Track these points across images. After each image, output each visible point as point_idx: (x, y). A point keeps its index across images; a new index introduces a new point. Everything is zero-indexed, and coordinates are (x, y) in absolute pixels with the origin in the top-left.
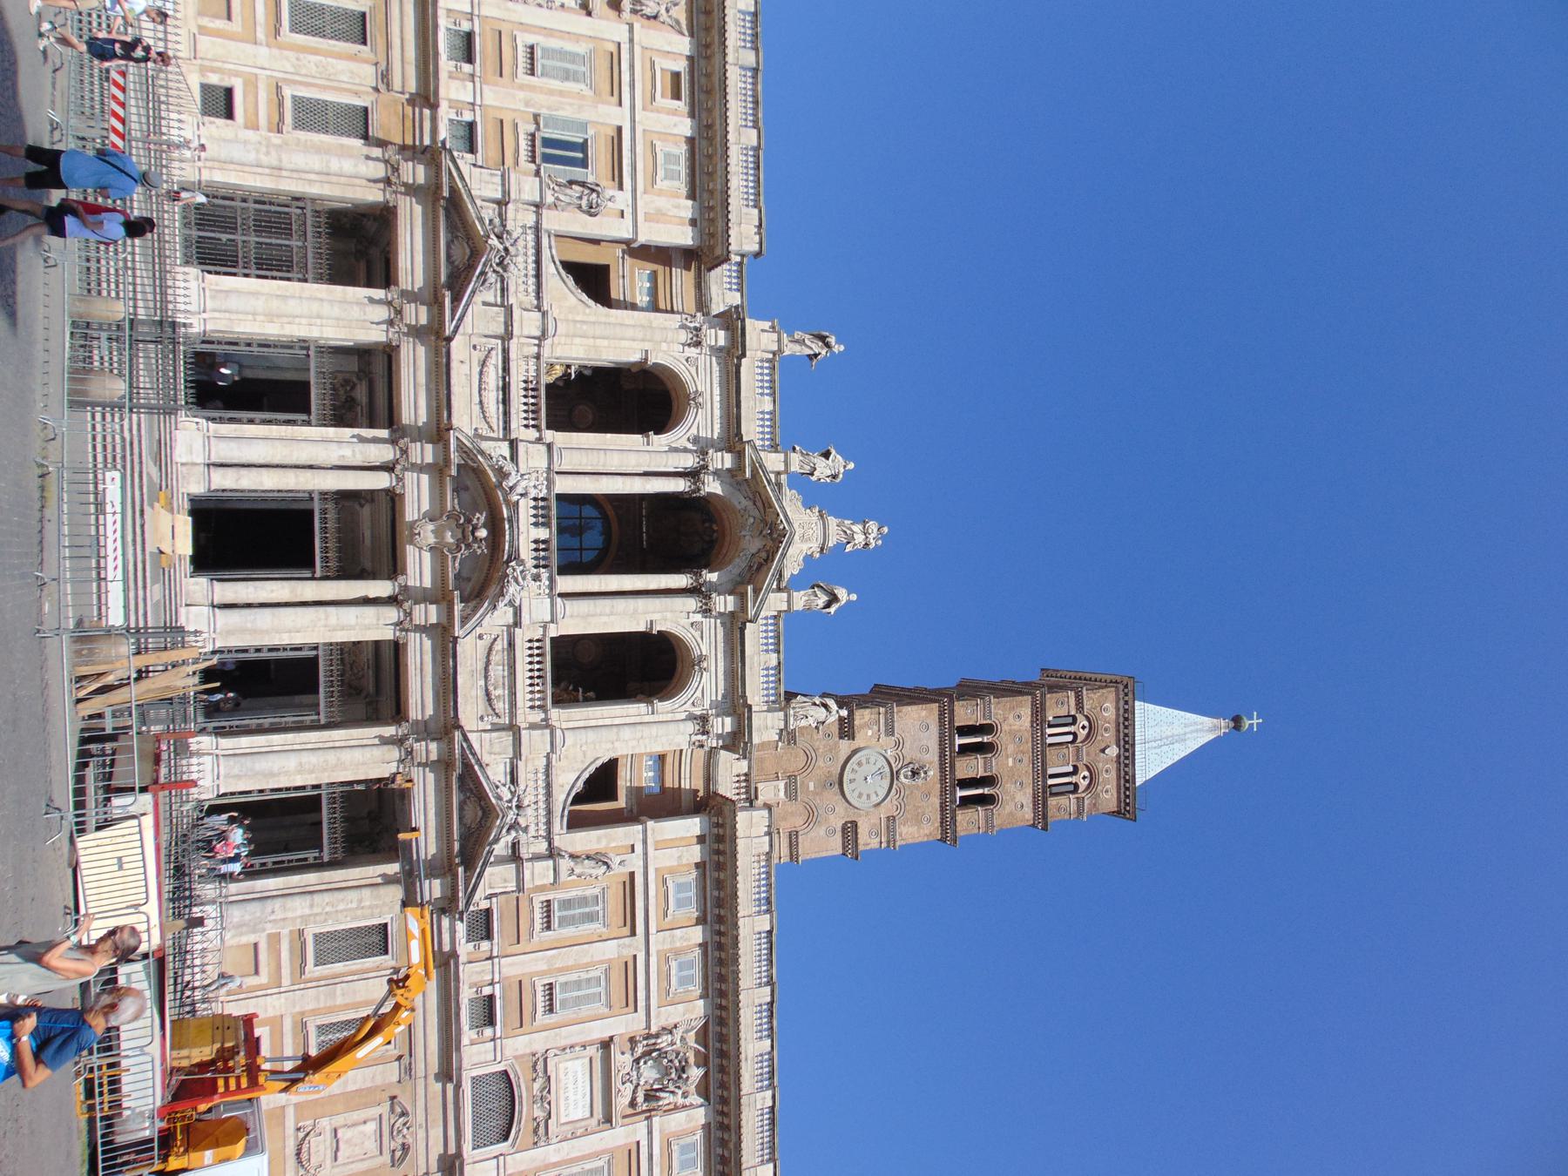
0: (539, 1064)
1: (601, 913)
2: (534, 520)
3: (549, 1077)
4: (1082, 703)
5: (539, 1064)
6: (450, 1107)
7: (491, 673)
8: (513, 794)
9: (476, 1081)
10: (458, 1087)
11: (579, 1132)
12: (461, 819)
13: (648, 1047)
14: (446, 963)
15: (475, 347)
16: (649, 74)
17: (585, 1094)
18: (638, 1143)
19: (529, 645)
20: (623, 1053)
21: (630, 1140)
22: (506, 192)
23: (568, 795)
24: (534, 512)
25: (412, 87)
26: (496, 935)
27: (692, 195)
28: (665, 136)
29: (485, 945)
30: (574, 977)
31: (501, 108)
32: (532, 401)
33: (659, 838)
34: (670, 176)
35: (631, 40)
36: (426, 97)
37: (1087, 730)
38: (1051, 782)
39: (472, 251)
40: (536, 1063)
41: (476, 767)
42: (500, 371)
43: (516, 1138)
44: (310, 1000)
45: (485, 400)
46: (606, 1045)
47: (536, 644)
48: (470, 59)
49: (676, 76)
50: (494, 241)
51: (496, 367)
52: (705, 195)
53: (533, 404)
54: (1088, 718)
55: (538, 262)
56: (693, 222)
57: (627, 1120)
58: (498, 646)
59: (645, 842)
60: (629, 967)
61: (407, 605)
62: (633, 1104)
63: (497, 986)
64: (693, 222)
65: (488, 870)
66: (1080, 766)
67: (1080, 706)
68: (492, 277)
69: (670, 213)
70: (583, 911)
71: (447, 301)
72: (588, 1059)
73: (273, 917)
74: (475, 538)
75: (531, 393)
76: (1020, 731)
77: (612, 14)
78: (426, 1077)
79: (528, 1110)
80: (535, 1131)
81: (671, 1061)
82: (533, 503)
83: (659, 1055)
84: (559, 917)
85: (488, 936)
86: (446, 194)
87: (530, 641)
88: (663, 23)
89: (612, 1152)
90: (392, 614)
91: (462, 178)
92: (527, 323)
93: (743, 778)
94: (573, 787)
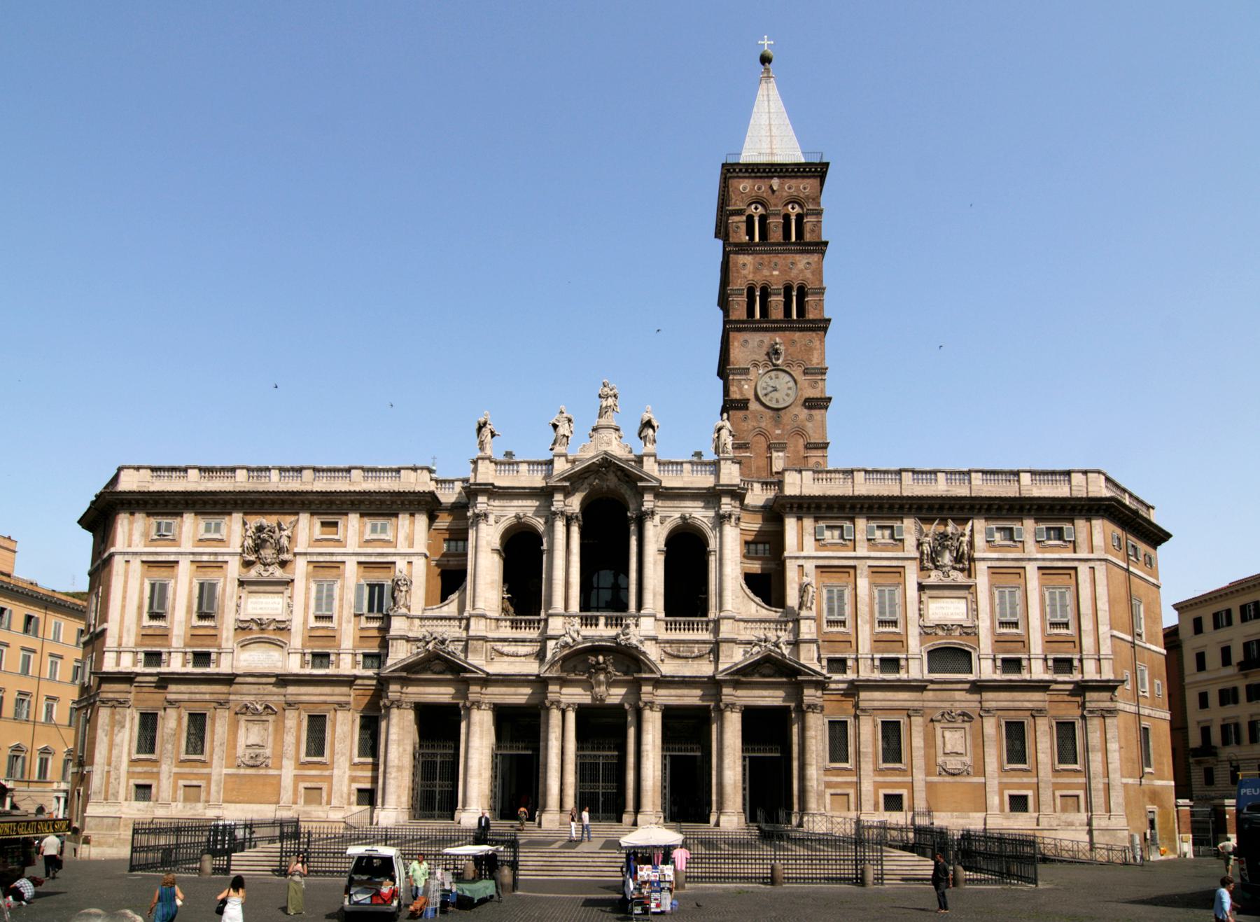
0: (926, 632)
1: (839, 588)
2: (594, 627)
3: (937, 625)
4: (738, 210)
5: (926, 632)
6: (944, 686)
7: (684, 654)
8: (756, 645)
9: (930, 671)
10: (932, 682)
11: (975, 607)
12: (769, 676)
13: (929, 560)
14: (854, 689)
15: (492, 659)
16: (324, 543)
17: (952, 603)
18: (988, 567)
19: (669, 631)
20: (930, 576)
21: (986, 573)
22: (402, 638)
23: (763, 607)
24: (589, 627)
25: (345, 690)
26: (844, 656)
27: (396, 515)
28: (362, 533)
29: (850, 663)
30: (876, 608)
31: (354, 638)
32: (523, 624)
33: (796, 548)
34: (384, 530)
35: (305, 554)
36: (349, 681)
37: (760, 207)
38: (793, 239)
39: (437, 659)
40: (927, 634)
41: (739, 666)
42: (506, 644)
43: (971, 647)
44: (867, 766)
45: (523, 653)
46: (921, 587)
47: (669, 626)
48: (328, 655)
49: (324, 524)
50: (430, 646)
51: (503, 646)
52: (395, 507)
53: (526, 624)
54: (750, 205)
55: (442, 618)
56: (412, 515)
57: (973, 575)
58: (669, 650)
59: (797, 558)
60: (875, 571)
61: (641, 704)
62: (962, 570)
63: (875, 656)
64: (412, 515)
65: (802, 661)
66: (783, 212)
67: (739, 212)
68: (451, 648)
69: (408, 531)
70: (836, 601)
71: (468, 675)
72: (930, 600)
73: (815, 786)
74: (604, 662)
75: (519, 625)
76: (754, 265)
77: (292, 566)
78: (923, 701)
79: (955, 639)
80: (967, 634)
81: (940, 544)
82: (584, 627)
83: (936, 552)
84: (838, 615)
85: (843, 662)
86: (404, 674)
87: (667, 630)
88: (292, 532)
89: (992, 586)
90: (647, 714)
91: (395, 664)
92: (477, 628)
93: (765, 487)
94: (758, 604)
